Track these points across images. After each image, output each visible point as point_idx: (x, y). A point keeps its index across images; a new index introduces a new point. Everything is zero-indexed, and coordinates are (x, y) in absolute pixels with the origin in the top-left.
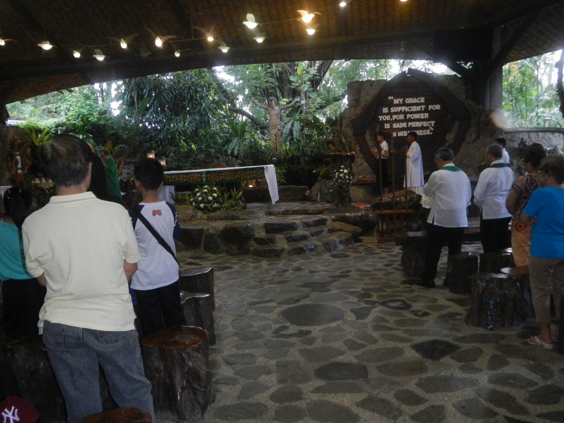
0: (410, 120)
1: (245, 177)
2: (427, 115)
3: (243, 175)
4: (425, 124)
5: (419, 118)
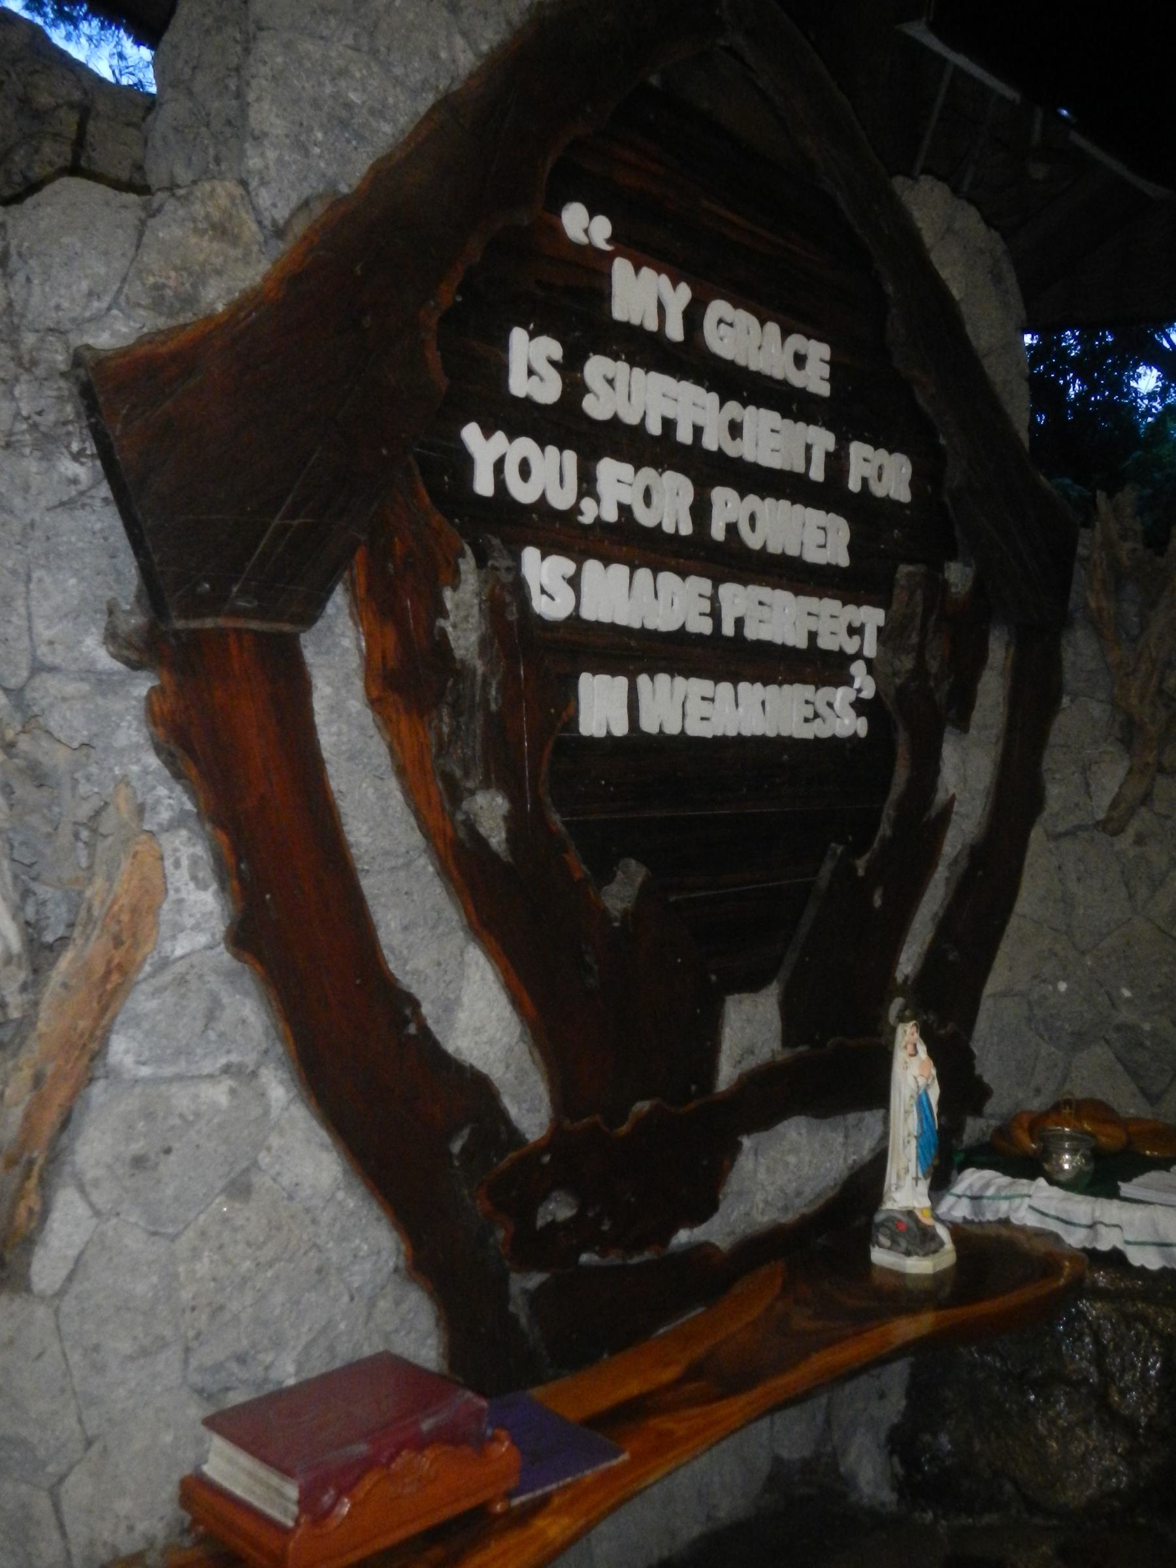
5: (793, 551)
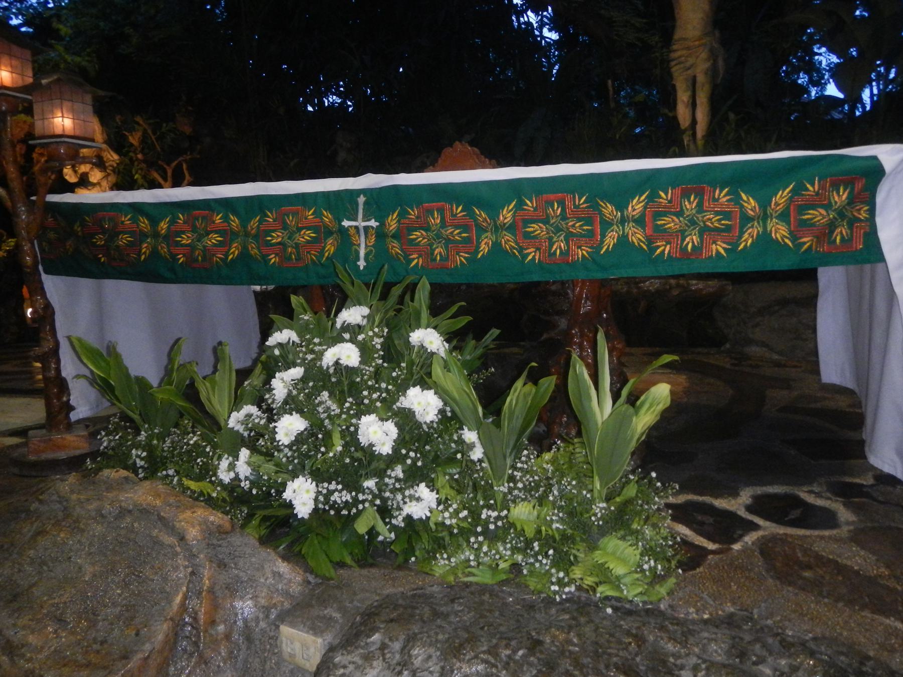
1: (692, 240)
3: (671, 223)
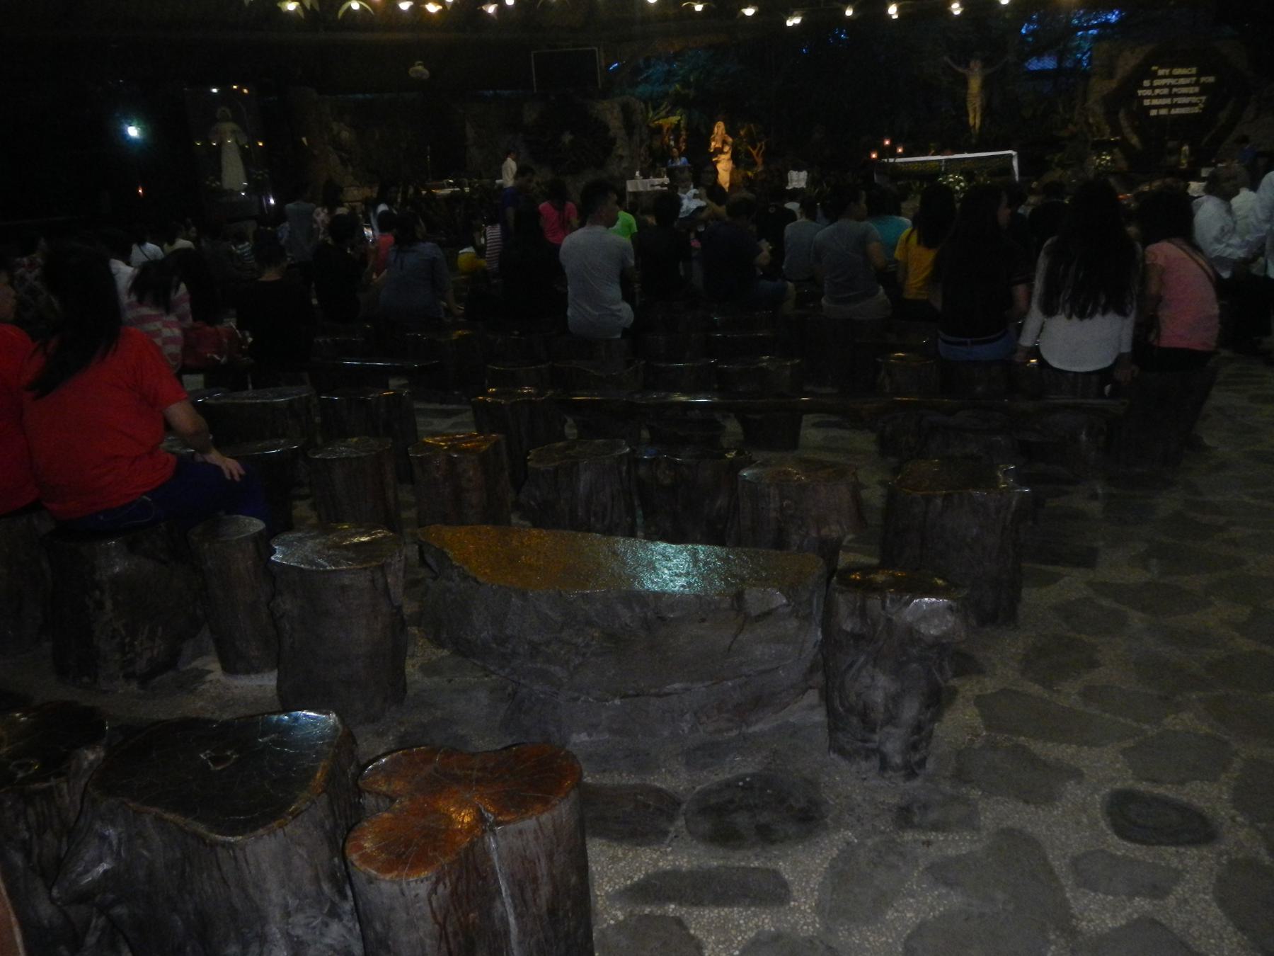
0: (1177, 95)
2: (1197, 89)
4: (1194, 99)
